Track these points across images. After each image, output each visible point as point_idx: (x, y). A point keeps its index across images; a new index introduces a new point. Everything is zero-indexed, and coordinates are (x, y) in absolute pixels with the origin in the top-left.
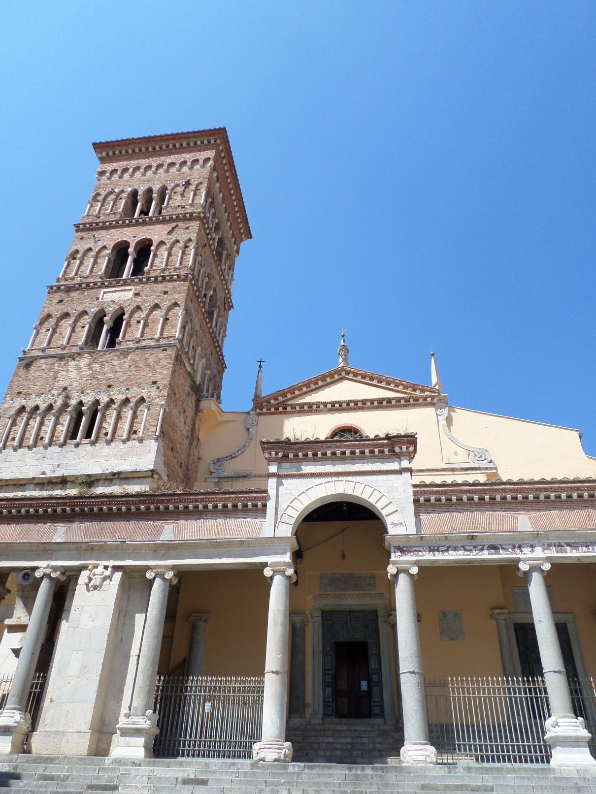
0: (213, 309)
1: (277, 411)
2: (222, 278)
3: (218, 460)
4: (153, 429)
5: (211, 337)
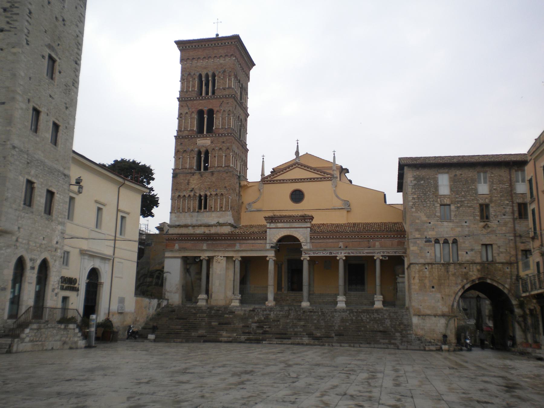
3: (249, 204)
4: (227, 207)
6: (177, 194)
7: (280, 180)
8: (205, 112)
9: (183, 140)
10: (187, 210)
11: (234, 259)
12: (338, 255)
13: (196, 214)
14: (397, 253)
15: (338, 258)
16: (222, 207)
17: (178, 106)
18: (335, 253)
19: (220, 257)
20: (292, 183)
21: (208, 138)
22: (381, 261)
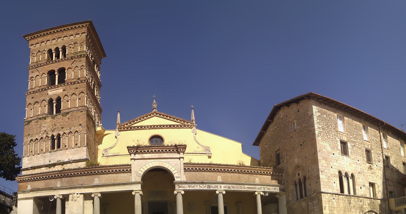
12: (217, 189)
15: (217, 192)
18: (214, 186)
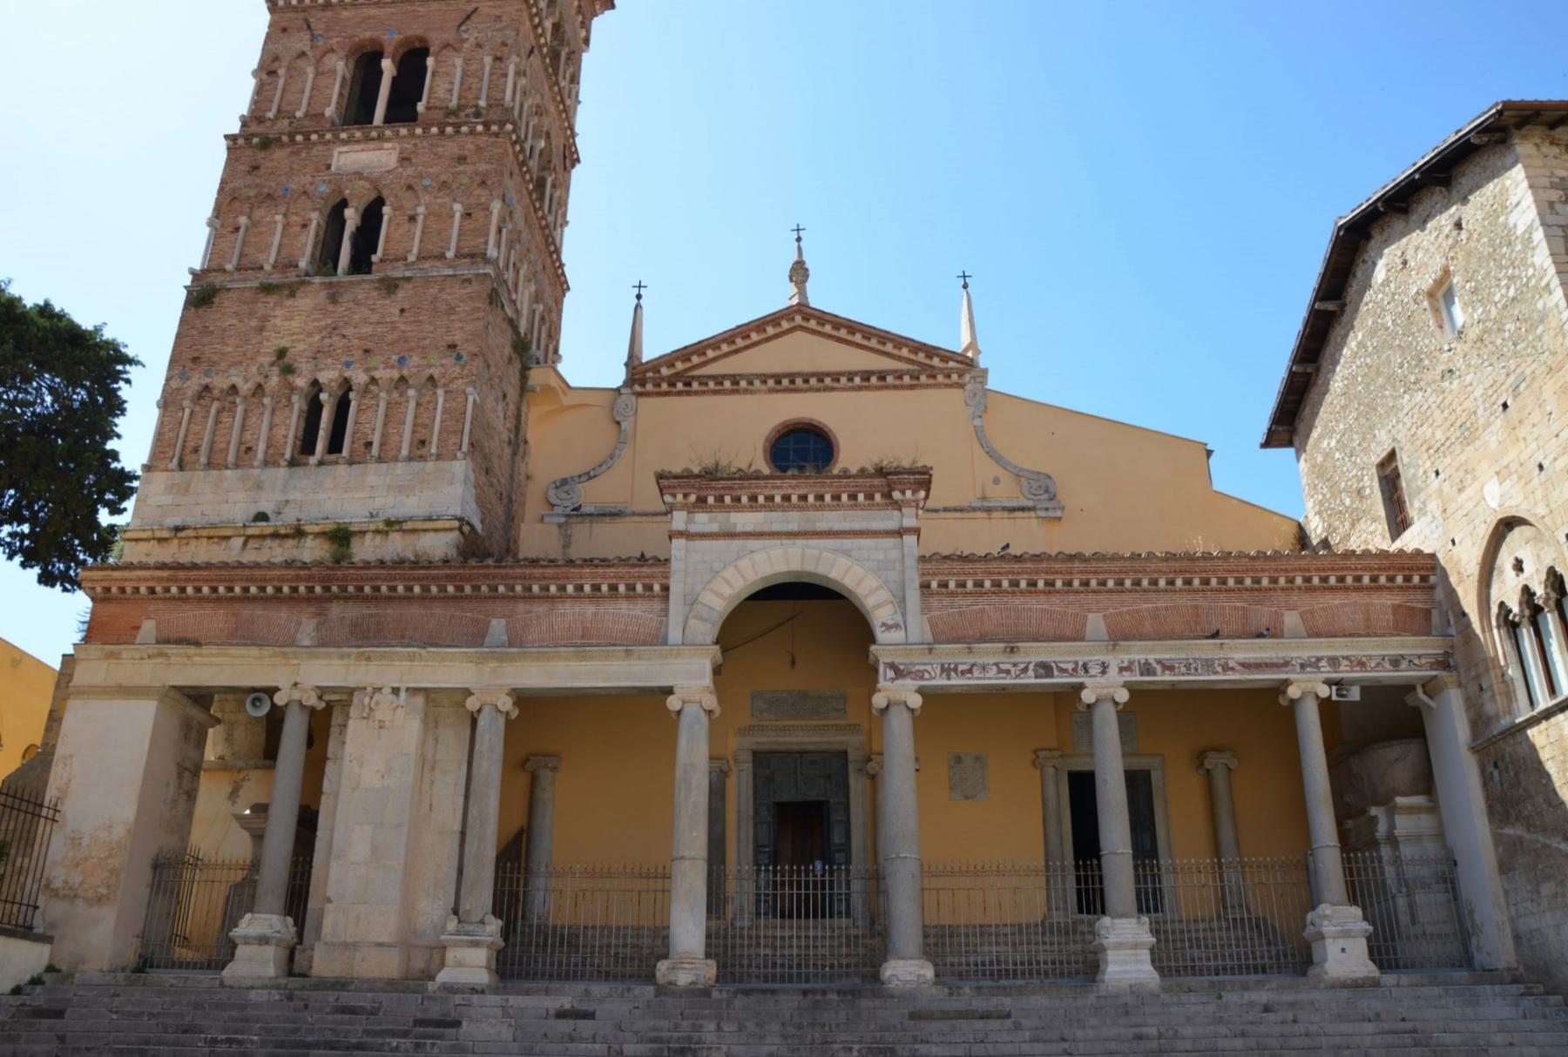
0: (545, 174)
1: (673, 389)
2: (561, 107)
3: (564, 482)
4: (454, 439)
5: (544, 235)
6: (195, 382)
7: (719, 379)
8: (388, 50)
9: (261, 155)
10: (238, 457)
11: (472, 704)
12: (1087, 681)
13: (282, 472)
14: (1404, 664)
15: (1088, 696)
16: (423, 442)
17: (263, 29)
18: (1070, 667)
19: (387, 691)
20: (778, 391)
21: (387, 145)
22: (1325, 705)
